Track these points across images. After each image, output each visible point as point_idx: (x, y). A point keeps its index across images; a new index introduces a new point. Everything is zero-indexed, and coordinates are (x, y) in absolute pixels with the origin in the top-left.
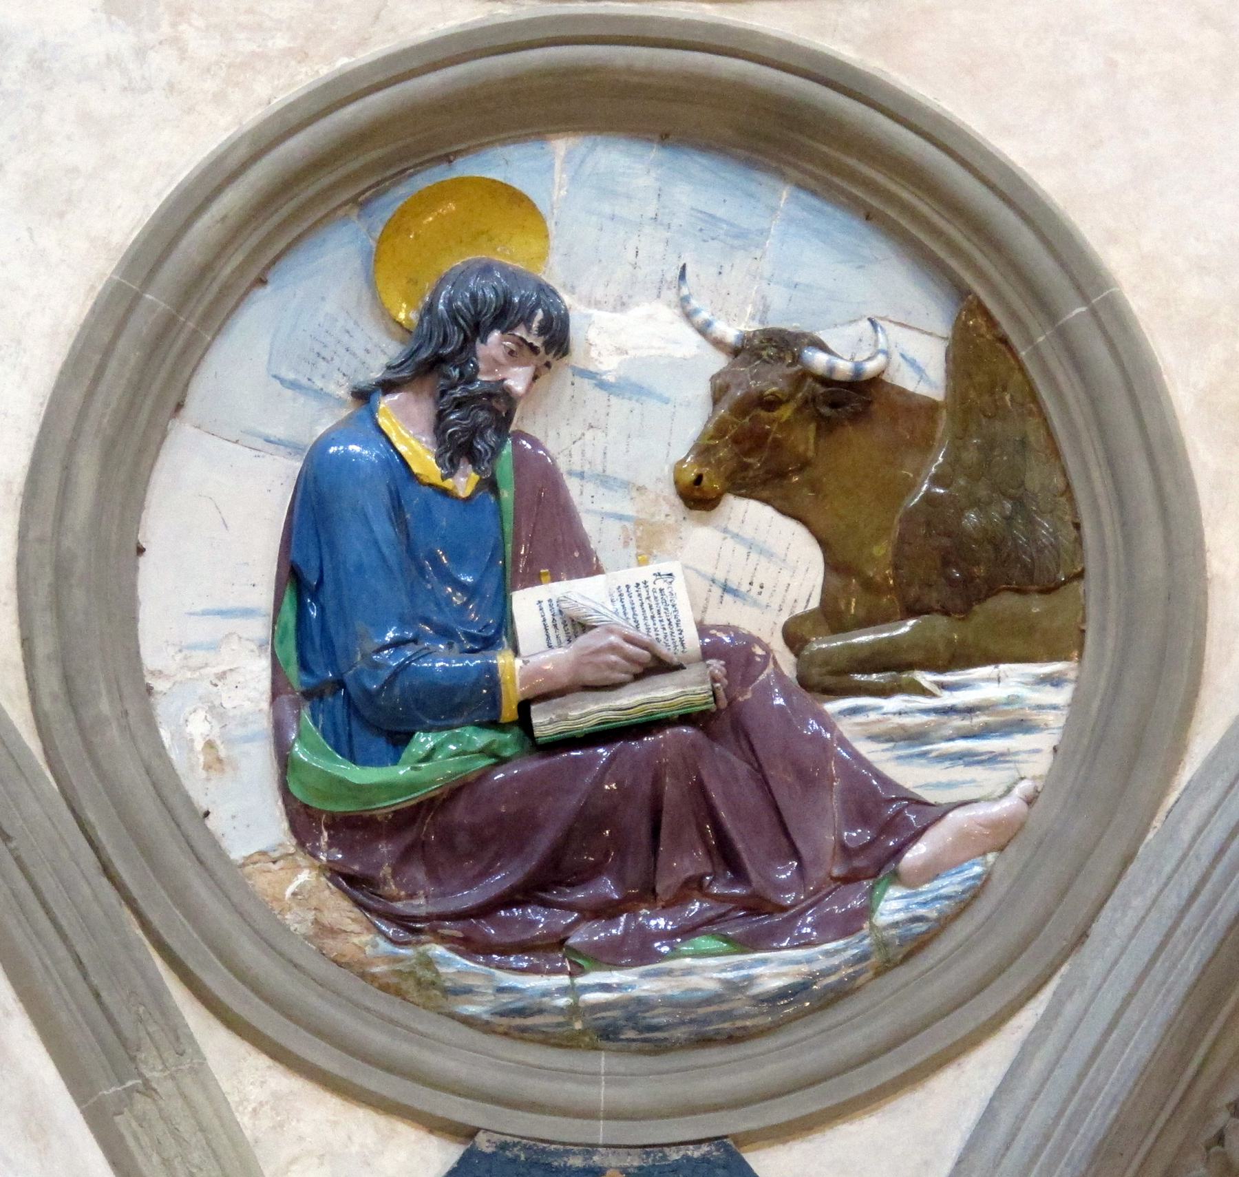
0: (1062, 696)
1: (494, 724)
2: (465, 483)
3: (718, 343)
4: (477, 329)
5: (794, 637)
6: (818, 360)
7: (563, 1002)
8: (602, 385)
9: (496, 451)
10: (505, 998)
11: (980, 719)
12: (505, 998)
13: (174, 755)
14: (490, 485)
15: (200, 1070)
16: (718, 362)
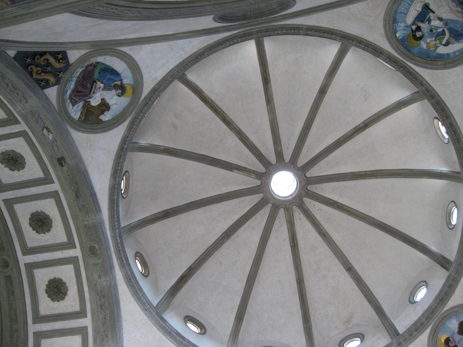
0: (75, 118)
1: (96, 80)
2: (113, 85)
3: (111, 105)
4: (122, 91)
5: (90, 102)
6: (106, 112)
7: (75, 76)
8: (113, 96)
9: (113, 88)
10: (78, 72)
11: (77, 112)
12: (78, 72)
13: (107, 56)
14: (111, 86)
15: (88, 49)
16: (110, 104)
